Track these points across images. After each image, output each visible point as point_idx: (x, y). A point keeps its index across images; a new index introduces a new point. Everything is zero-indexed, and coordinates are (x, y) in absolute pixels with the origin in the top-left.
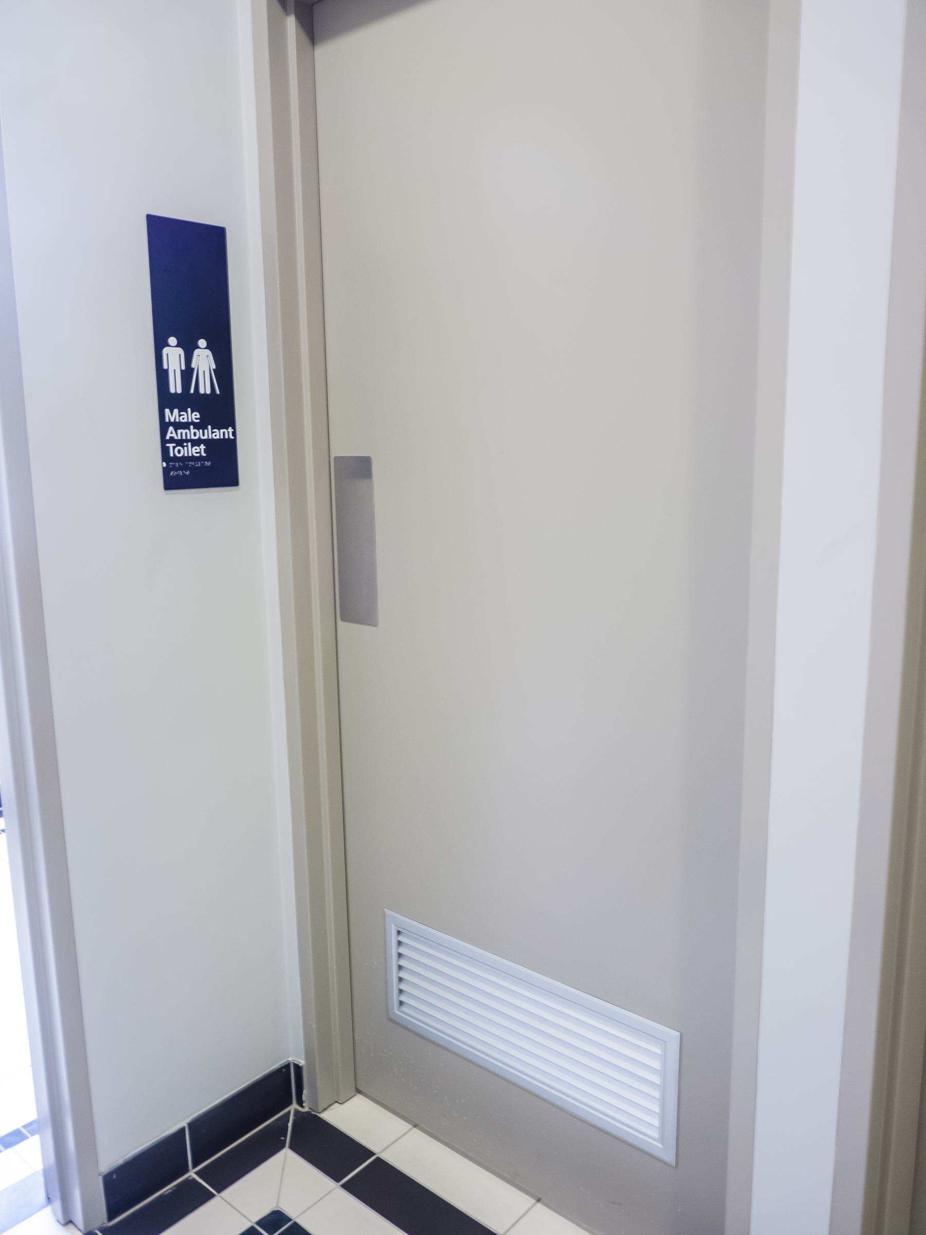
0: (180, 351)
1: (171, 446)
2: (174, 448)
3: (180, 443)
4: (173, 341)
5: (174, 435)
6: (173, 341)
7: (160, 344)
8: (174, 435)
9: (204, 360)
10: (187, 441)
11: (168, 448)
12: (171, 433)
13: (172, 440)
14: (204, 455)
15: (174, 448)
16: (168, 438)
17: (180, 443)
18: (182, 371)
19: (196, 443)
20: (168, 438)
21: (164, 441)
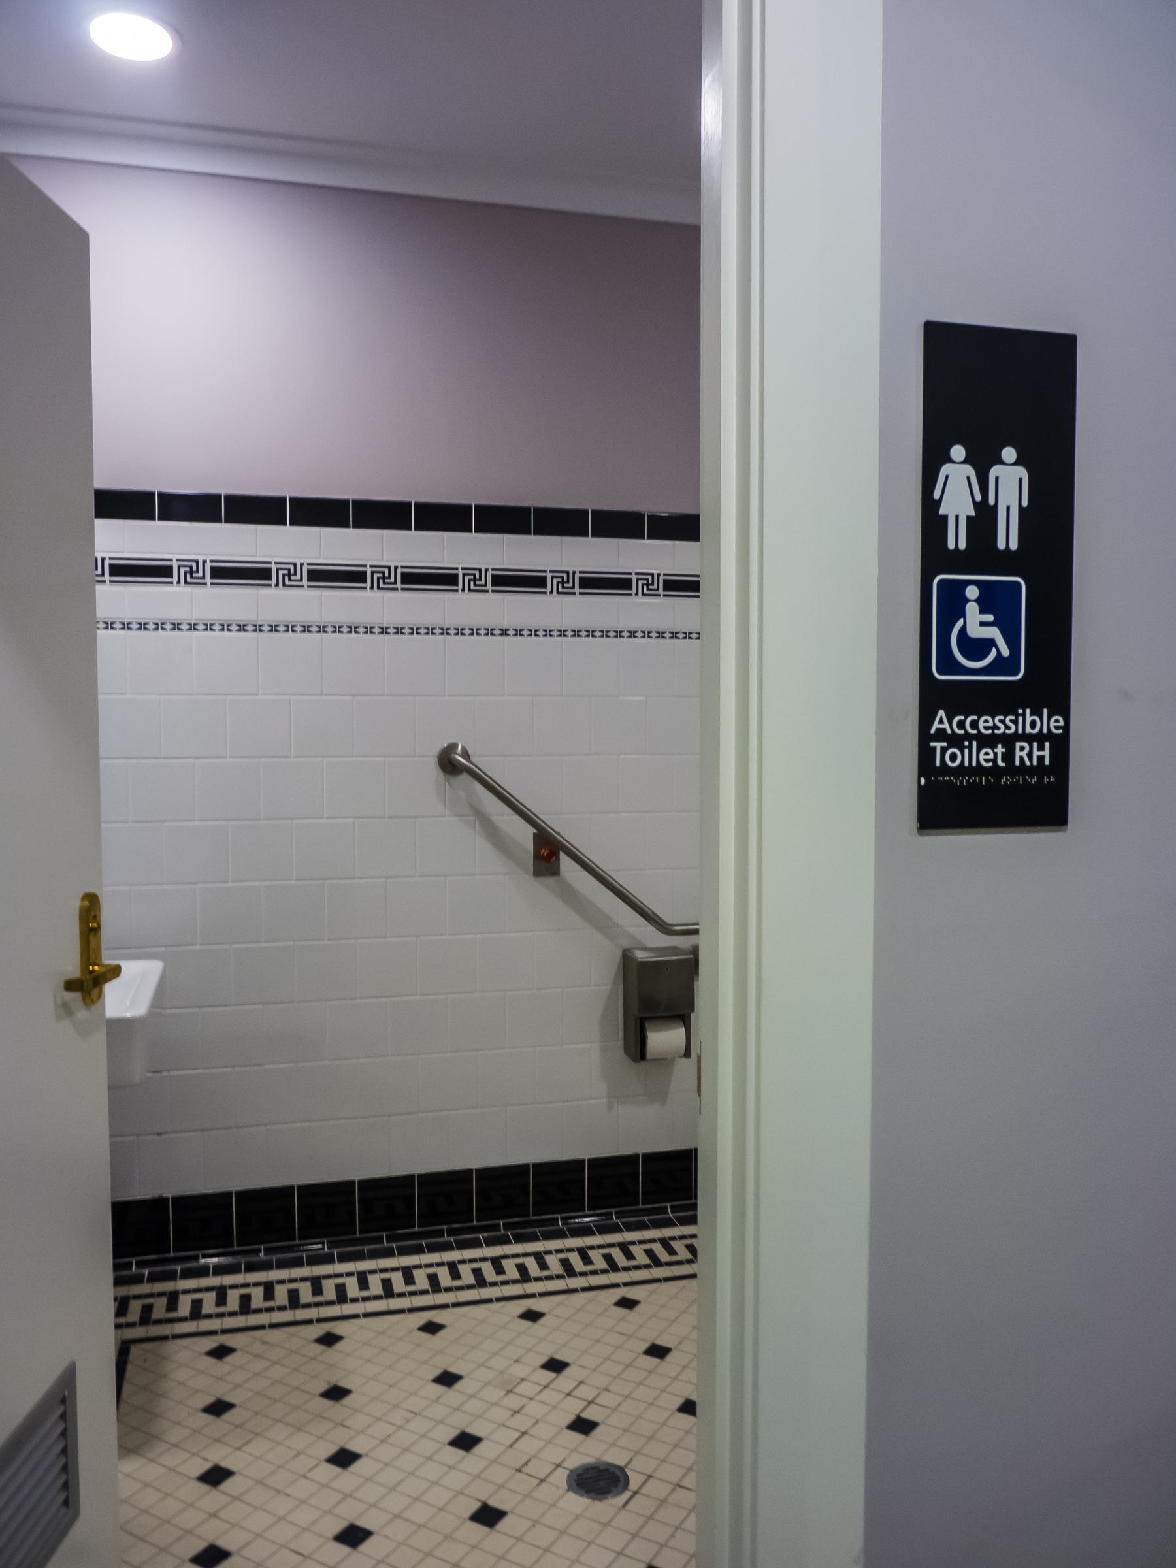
0: (969, 470)
1: (938, 745)
2: (944, 750)
3: (955, 741)
4: (958, 452)
5: (946, 725)
6: (958, 452)
7: (933, 460)
8: (946, 725)
9: (1011, 482)
10: (968, 736)
11: (935, 748)
12: (941, 721)
13: (941, 735)
14: (1001, 764)
15: (944, 750)
16: (933, 731)
17: (955, 741)
18: (969, 518)
19: (987, 741)
20: (936, 725)
21: (925, 737)
